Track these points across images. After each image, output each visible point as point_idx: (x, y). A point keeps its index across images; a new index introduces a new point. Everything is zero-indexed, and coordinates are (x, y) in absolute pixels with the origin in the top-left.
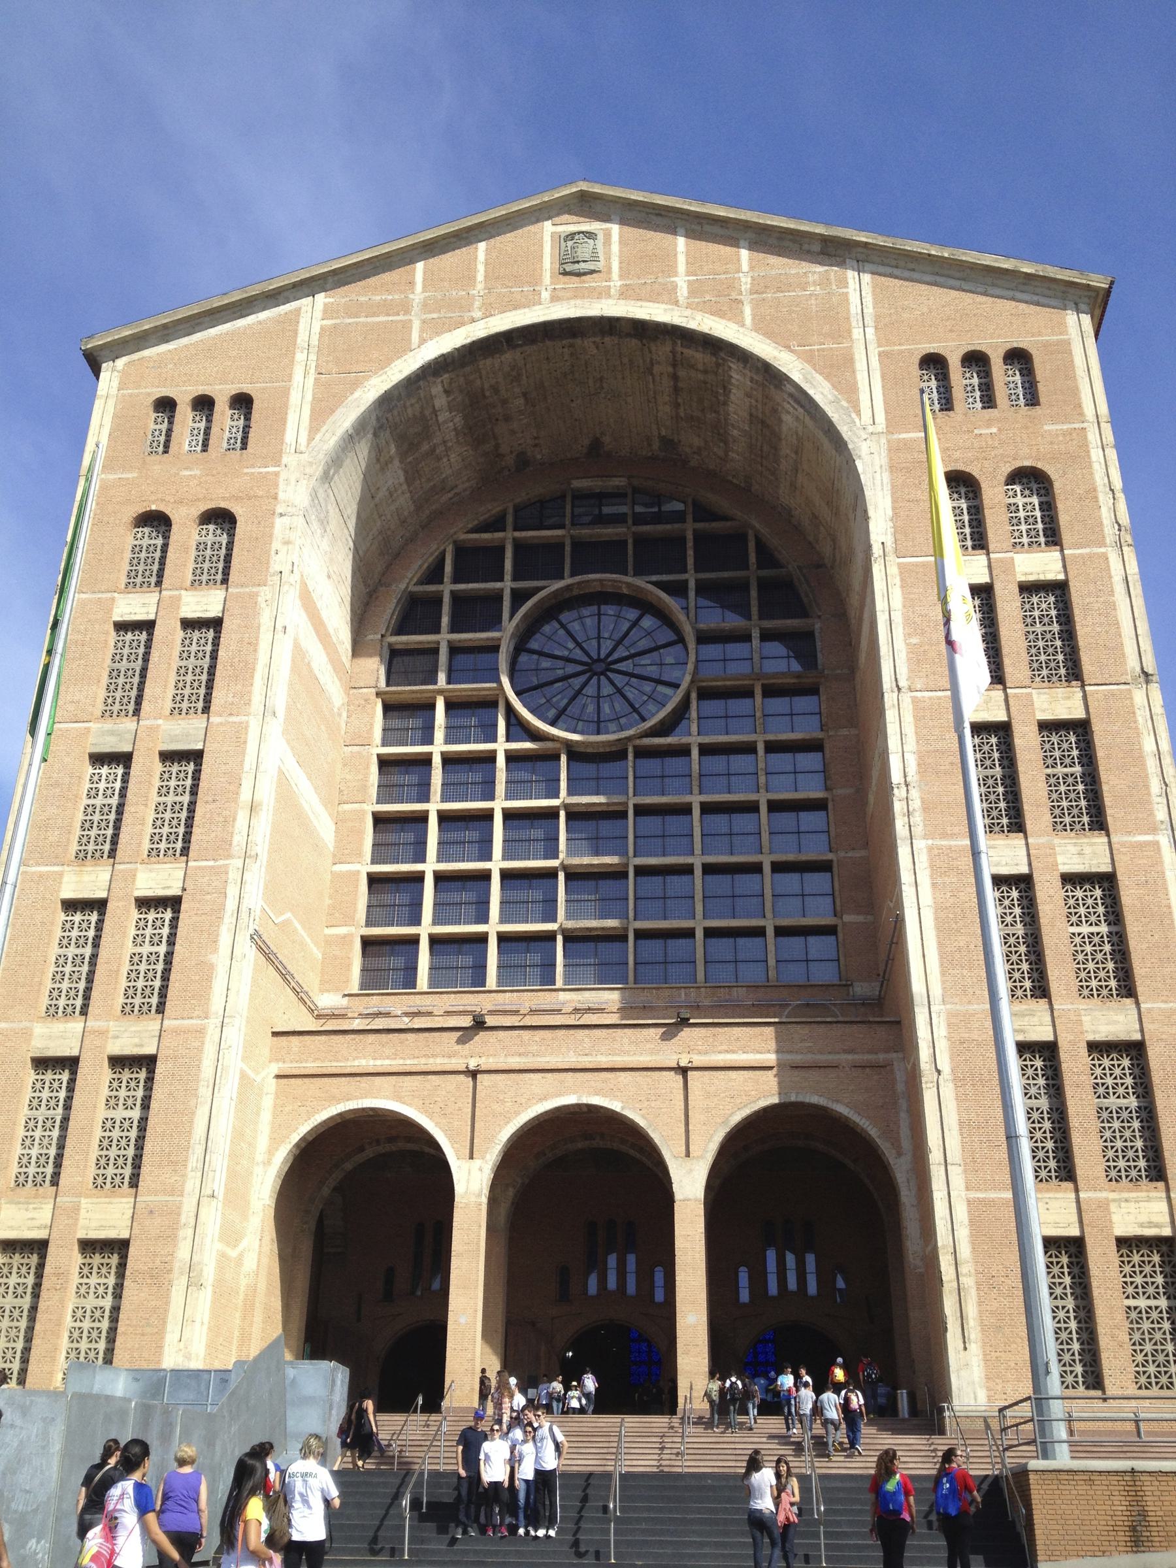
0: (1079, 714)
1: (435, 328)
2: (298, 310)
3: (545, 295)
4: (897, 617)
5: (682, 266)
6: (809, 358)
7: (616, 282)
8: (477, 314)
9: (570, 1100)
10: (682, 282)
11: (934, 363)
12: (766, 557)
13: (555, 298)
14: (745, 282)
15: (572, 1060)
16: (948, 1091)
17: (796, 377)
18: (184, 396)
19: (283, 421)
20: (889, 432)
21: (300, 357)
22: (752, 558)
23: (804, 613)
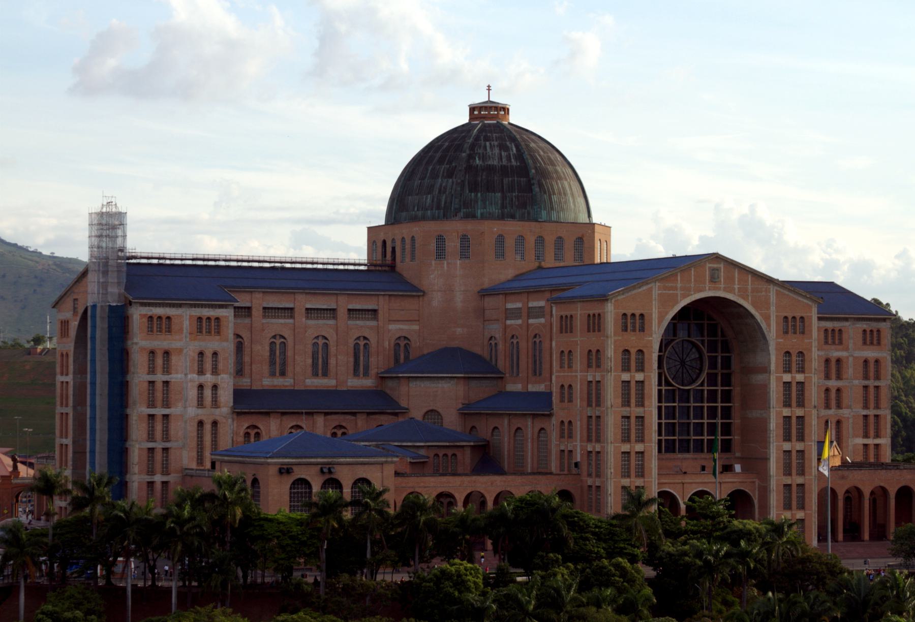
0: (803, 415)
1: (684, 296)
2: (652, 287)
3: (707, 288)
4: (775, 389)
5: (736, 283)
6: (761, 314)
7: (722, 286)
8: (692, 293)
9: (700, 489)
10: (736, 287)
11: (786, 317)
12: (723, 335)
13: (709, 289)
14: (750, 287)
15: (700, 480)
16: (775, 493)
17: (759, 321)
18: (629, 313)
19: (652, 323)
20: (776, 339)
21: (654, 303)
22: (720, 333)
23: (729, 352)
